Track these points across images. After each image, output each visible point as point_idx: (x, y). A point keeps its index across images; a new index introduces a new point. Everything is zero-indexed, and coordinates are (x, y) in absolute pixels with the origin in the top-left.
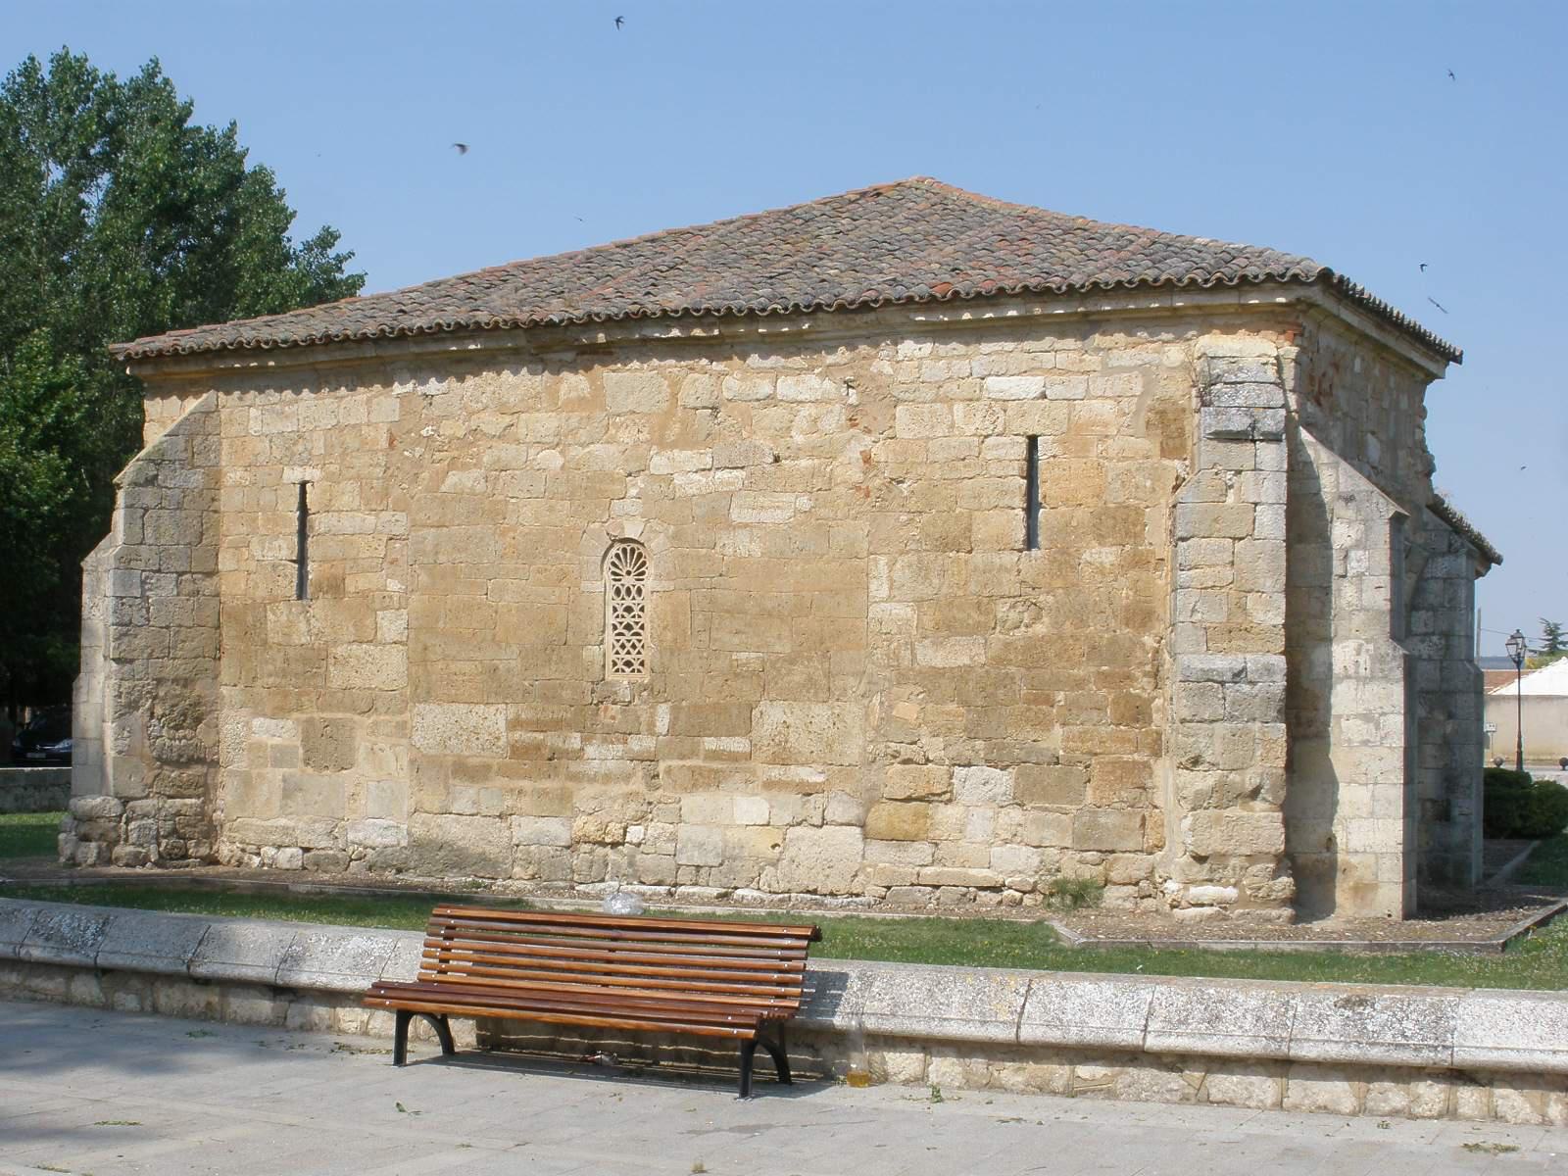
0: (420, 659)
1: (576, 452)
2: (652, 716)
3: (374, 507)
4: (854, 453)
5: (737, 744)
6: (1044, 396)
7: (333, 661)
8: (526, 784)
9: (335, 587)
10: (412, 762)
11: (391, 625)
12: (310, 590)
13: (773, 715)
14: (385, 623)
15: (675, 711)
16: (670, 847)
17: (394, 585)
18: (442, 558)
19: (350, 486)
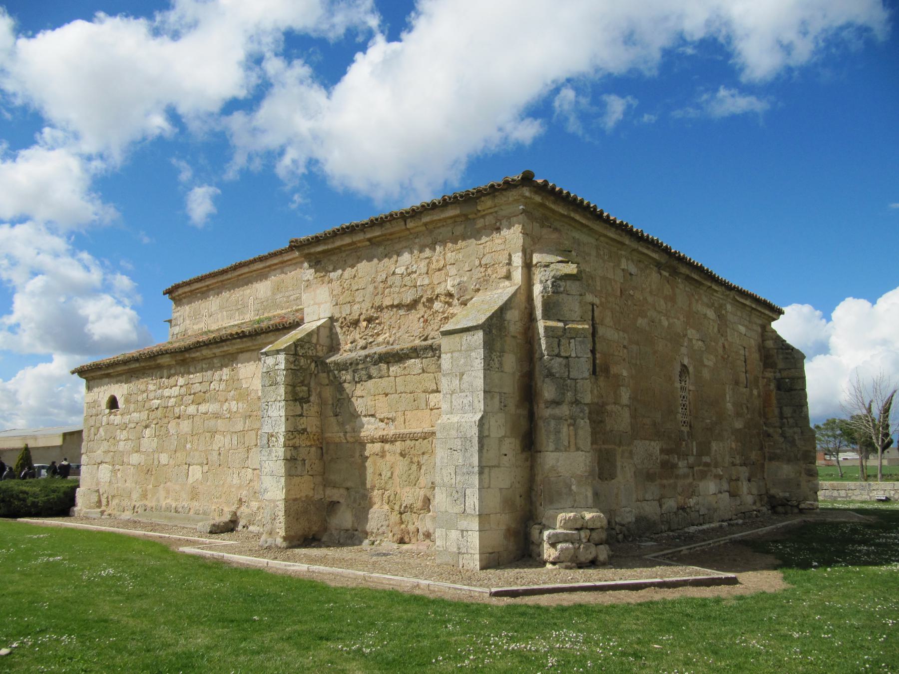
0: (633, 416)
1: (671, 321)
2: (692, 446)
3: (617, 327)
4: (720, 344)
5: (706, 459)
6: (745, 335)
7: (606, 414)
8: (665, 482)
9: (606, 370)
10: (635, 472)
11: (625, 396)
12: (598, 369)
13: (714, 446)
14: (623, 394)
15: (697, 443)
16: (697, 507)
17: (625, 373)
18: (638, 363)
19: (609, 313)
